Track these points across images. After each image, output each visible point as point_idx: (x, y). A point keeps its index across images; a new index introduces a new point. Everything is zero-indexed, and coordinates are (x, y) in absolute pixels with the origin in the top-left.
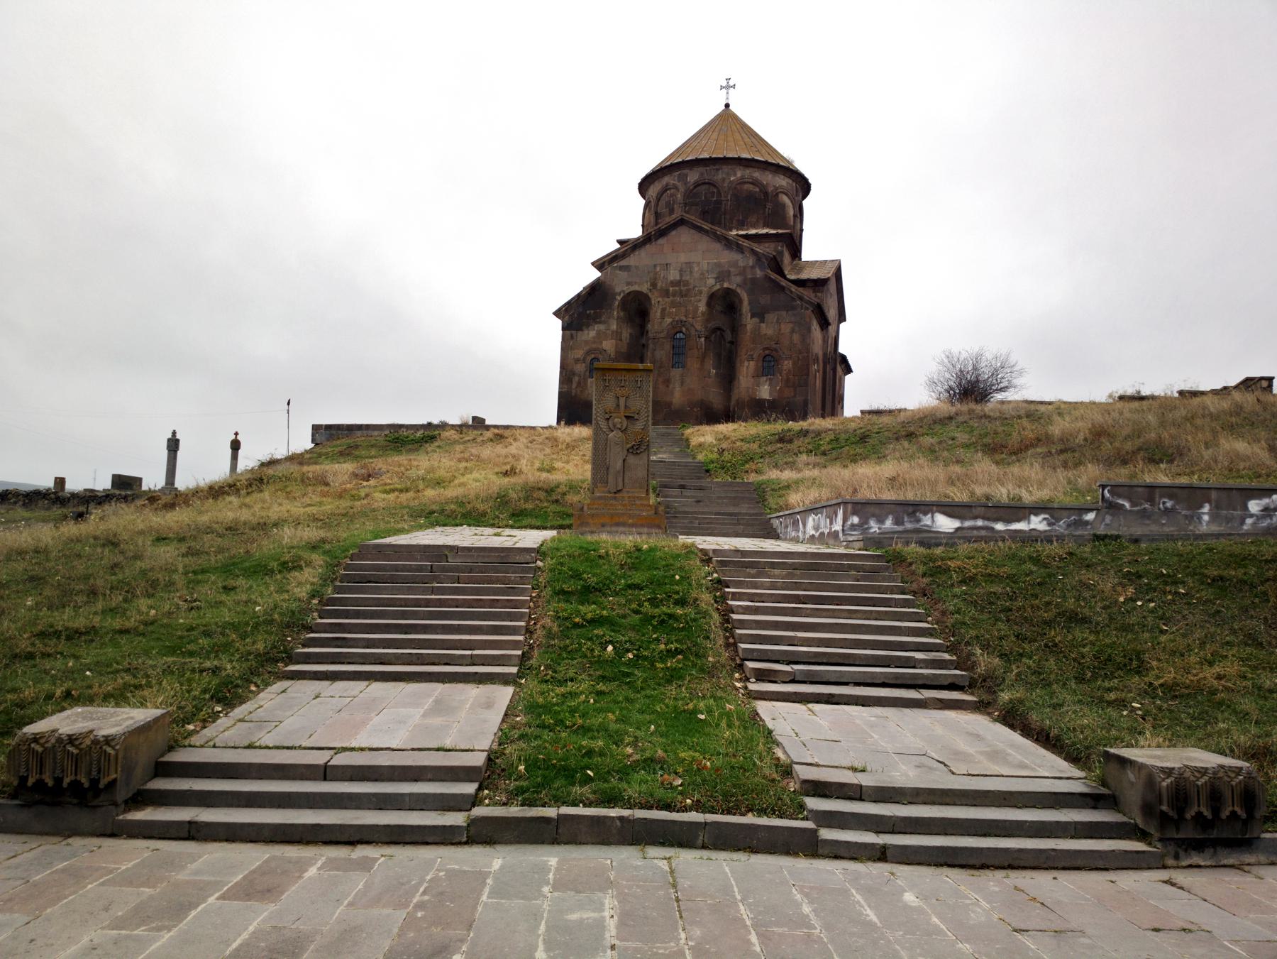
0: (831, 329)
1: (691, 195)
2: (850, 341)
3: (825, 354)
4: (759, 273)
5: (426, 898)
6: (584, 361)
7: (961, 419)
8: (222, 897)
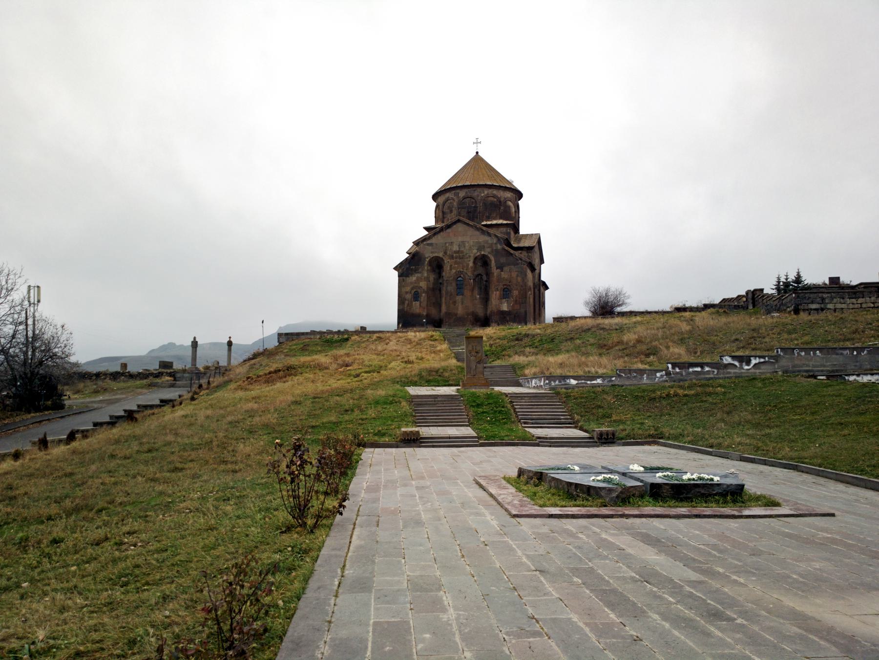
0: (537, 271)
1: (461, 204)
2: (547, 273)
4: (499, 247)
7: (593, 330)
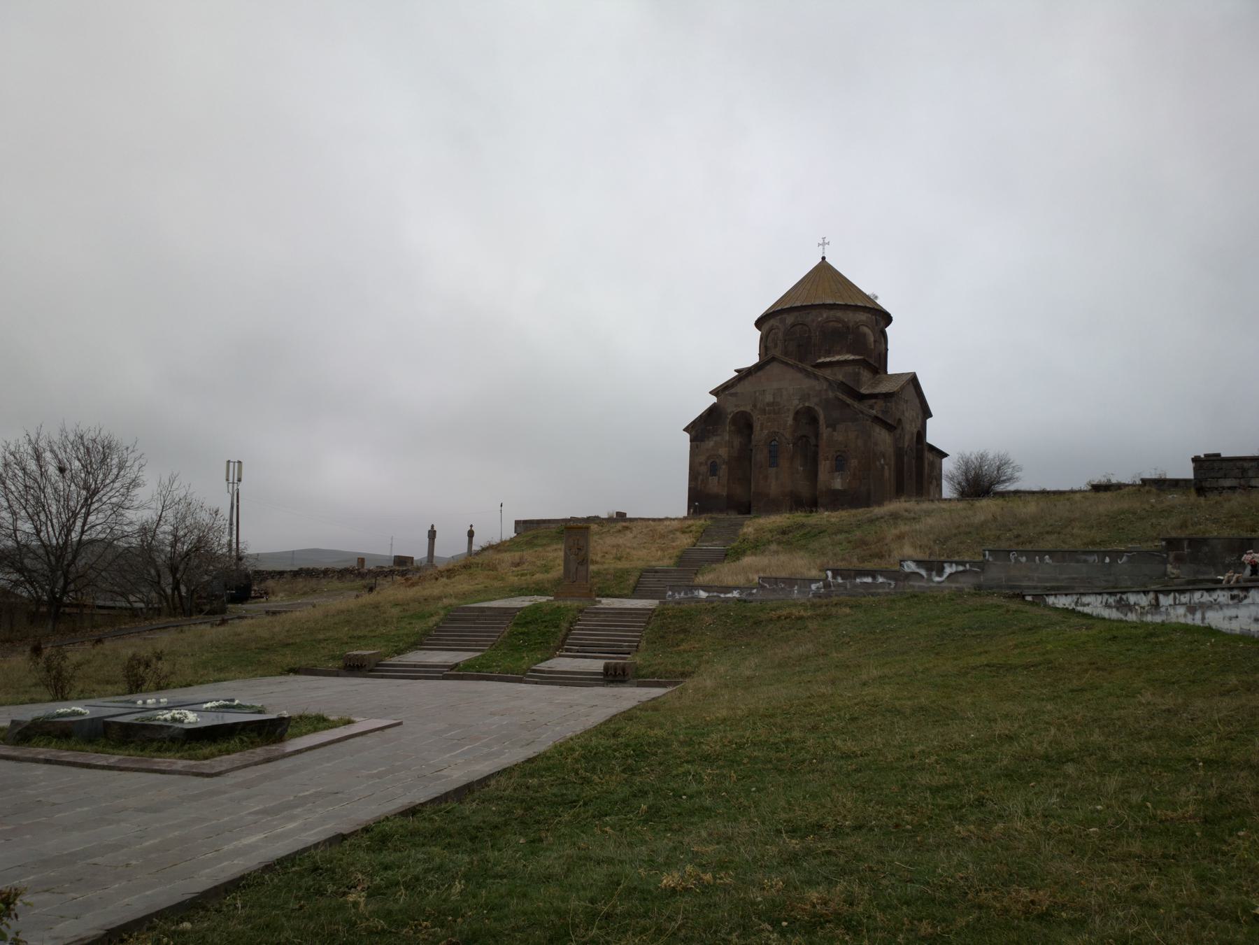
4: (831, 395)
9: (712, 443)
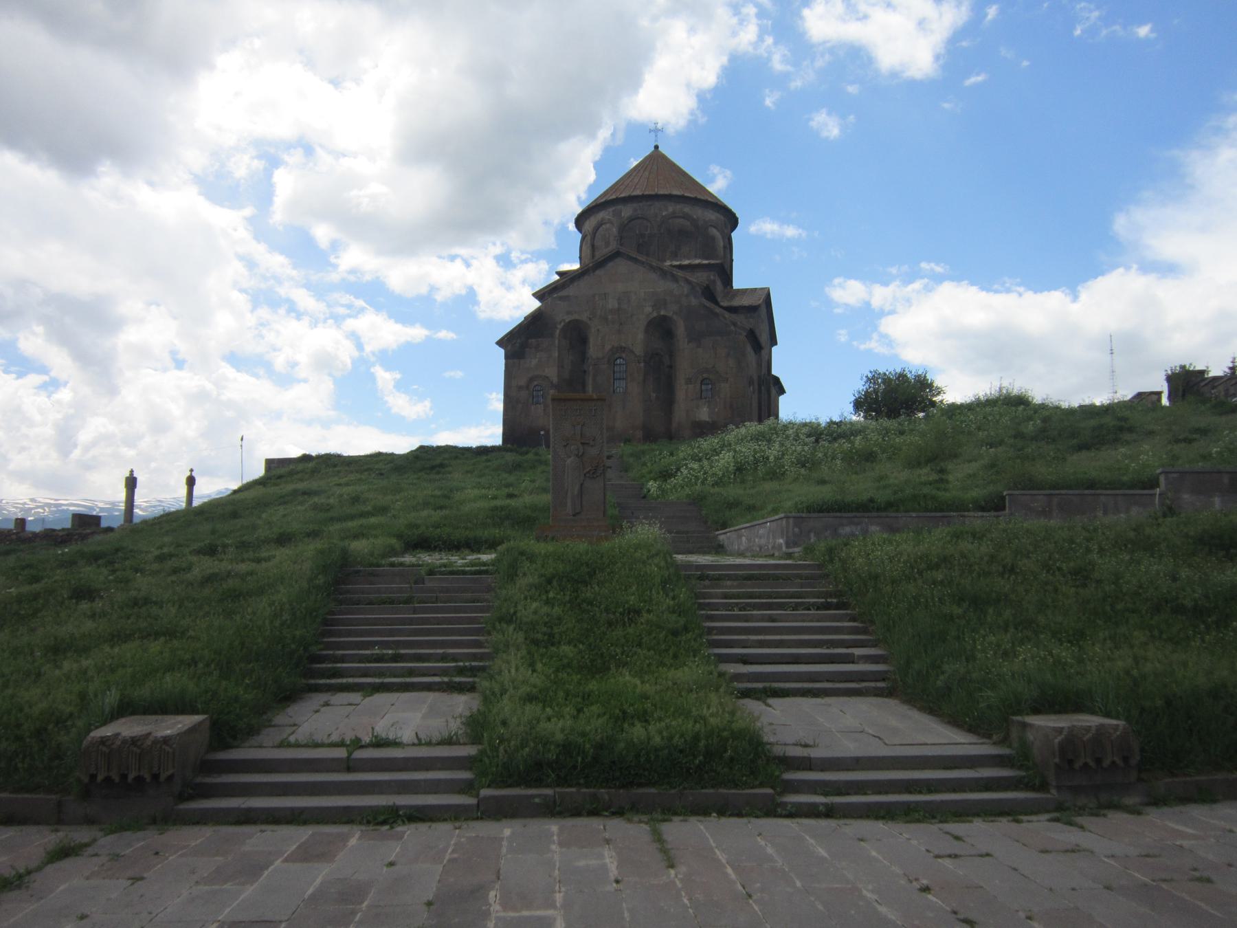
0: (764, 352)
2: (782, 363)
3: (759, 377)
4: (694, 302)
5: (455, 856)
6: (527, 387)
8: (286, 860)
9: (534, 362)
